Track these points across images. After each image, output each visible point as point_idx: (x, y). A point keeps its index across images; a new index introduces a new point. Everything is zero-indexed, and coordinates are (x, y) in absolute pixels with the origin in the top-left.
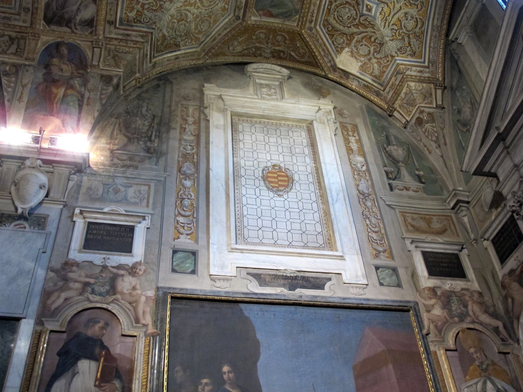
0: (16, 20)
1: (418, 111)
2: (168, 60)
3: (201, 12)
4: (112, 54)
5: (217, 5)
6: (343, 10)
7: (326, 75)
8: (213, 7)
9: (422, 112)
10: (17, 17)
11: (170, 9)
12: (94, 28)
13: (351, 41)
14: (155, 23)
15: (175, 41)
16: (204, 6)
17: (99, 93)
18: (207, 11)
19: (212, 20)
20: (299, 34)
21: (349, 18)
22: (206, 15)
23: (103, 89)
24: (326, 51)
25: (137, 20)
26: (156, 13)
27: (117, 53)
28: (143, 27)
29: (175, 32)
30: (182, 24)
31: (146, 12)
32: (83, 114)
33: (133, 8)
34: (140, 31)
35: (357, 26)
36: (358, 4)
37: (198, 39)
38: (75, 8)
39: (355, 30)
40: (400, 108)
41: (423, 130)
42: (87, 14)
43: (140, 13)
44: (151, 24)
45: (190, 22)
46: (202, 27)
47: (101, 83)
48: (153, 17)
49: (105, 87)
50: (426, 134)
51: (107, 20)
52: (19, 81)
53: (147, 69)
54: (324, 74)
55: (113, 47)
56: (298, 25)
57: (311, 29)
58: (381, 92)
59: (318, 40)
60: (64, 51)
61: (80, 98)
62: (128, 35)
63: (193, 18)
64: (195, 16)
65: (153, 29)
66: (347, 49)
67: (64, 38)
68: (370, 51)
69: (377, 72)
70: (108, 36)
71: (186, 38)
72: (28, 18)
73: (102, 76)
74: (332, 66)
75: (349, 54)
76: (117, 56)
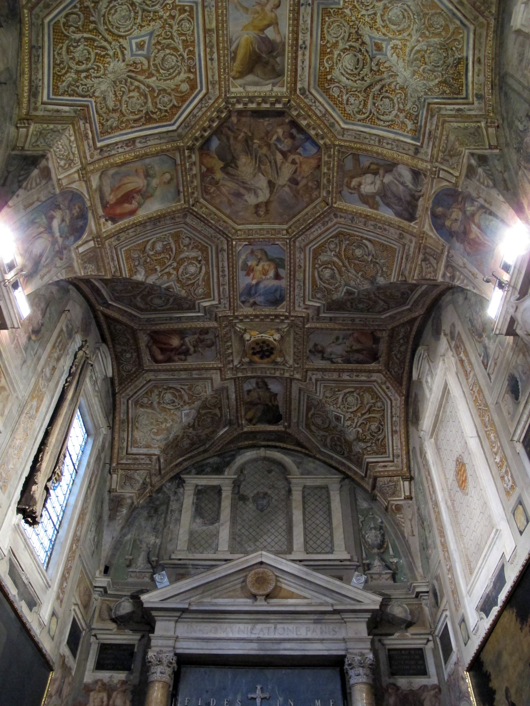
0: (409, 249)
2: (478, 76)
3: (417, 31)
4: (447, 158)
5: (408, 6)
8: (412, 12)
10: (407, 247)
11: (405, 77)
12: (421, 172)
14: (419, 98)
15: (452, 67)
16: (409, 26)
17: (482, 187)
18: (417, 21)
19: (431, 12)
22: (423, 21)
23: (479, 180)
25: (415, 119)
26: (409, 95)
27: (447, 152)
28: (422, 114)
29: (438, 66)
30: (429, 57)
31: (407, 108)
32: (499, 214)
33: (403, 122)
34: (426, 118)
37: (456, 31)
38: (401, 188)
42: (407, 176)
43: (409, 116)
44: (420, 102)
45: (428, 46)
46: (438, 26)
47: (473, 179)
48: (413, 99)
49: (478, 177)
51: (412, 154)
52: (460, 269)
53: (481, 109)
60: (440, 210)
61: (484, 210)
62: (430, 132)
63: (423, 41)
64: (420, 39)
65: (425, 101)
67: (427, 208)
70: (429, 157)
71: (452, 49)
73: (467, 176)
76: (449, 151)
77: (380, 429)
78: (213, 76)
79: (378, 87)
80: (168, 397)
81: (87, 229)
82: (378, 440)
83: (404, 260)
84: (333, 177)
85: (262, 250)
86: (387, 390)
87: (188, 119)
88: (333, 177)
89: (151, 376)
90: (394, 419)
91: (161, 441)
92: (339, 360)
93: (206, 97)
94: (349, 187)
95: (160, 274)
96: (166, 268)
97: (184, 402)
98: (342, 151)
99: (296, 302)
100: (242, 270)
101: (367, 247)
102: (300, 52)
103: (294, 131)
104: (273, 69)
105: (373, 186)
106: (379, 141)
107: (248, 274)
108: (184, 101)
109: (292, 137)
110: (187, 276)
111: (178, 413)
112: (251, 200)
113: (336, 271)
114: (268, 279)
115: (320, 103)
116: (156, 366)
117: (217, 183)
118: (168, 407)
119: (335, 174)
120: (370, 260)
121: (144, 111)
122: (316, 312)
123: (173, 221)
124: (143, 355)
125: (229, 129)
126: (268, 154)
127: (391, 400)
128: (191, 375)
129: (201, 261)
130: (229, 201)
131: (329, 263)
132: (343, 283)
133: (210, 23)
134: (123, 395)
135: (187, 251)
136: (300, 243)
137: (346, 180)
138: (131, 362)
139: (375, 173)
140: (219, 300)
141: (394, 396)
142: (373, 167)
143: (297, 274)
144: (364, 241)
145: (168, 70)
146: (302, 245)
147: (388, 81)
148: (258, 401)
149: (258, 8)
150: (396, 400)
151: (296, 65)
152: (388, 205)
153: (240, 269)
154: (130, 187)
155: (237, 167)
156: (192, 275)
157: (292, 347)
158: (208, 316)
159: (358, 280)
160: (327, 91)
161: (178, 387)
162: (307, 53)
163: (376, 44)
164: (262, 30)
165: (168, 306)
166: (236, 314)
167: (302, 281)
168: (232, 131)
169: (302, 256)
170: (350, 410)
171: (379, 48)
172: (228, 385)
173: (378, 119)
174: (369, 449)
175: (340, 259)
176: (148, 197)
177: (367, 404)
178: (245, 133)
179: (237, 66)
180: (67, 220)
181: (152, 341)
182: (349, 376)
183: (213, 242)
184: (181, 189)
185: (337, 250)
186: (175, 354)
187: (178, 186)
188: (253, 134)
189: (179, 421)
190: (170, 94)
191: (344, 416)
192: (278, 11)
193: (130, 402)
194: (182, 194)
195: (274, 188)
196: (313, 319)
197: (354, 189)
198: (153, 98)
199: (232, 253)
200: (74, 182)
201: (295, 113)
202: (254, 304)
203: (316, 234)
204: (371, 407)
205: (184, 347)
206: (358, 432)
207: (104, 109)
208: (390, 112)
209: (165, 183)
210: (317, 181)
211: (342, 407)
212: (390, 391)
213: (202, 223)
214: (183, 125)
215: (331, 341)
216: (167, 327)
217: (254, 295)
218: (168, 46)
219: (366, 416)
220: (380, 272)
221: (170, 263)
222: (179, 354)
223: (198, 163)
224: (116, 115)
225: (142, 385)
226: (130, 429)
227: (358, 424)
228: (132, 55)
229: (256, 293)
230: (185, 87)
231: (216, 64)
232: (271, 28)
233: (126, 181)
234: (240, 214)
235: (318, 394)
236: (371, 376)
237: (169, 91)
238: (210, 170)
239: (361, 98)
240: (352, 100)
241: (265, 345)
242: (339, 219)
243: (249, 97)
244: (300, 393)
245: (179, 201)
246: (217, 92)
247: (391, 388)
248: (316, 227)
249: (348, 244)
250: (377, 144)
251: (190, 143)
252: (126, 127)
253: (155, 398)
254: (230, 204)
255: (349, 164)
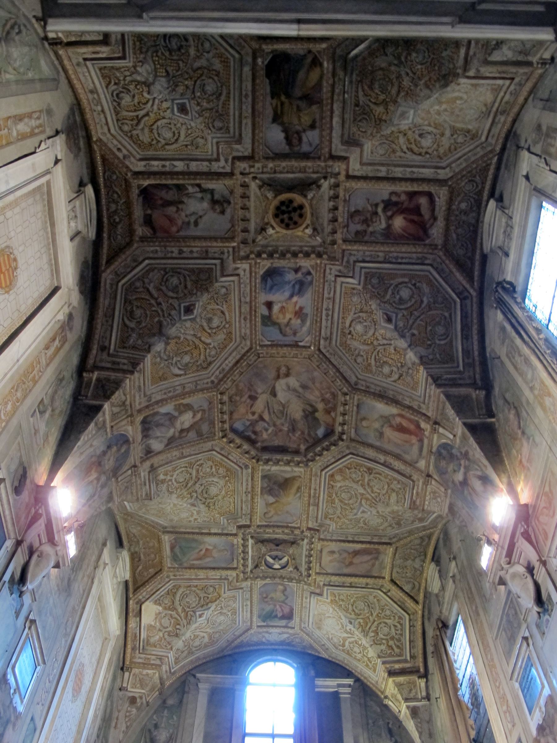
0: (140, 396)
1: (140, 695)
6: (193, 596)
7: (130, 599)
9: (141, 698)
10: (142, 396)
13: (169, 609)
14: (159, 496)
20: (161, 570)
21: (188, 602)
24: (152, 592)
31: (165, 485)
35: (183, 610)
36: (202, 606)
38: (158, 434)
39: (180, 610)
40: (134, 675)
41: (129, 709)
42: (156, 446)
43: (163, 482)
50: (128, 714)
54: (131, 596)
55: (134, 480)
56: (169, 568)
57: (168, 577)
58: (138, 651)
59: (159, 584)
62: (145, 485)
66: (160, 608)
67: (134, 443)
68: (167, 627)
69: (152, 640)
72: (143, 405)
74: (140, 600)
75: (158, 612)
77: (117, 98)
78: (316, 480)
79: (189, 485)
80: (427, 142)
81: (440, 443)
82: (115, 84)
83: (142, 386)
84: (218, 416)
85: (285, 335)
86: (119, 146)
87: (340, 457)
88: (218, 416)
89: (443, 174)
90: (99, 108)
91: (453, 91)
92: (191, 189)
93: (323, 467)
94: (204, 411)
95: (392, 342)
96: (384, 345)
97: (405, 135)
98: (211, 436)
99: (248, 275)
100: (307, 315)
101: (179, 369)
102: (250, 490)
103: (253, 437)
104: (270, 480)
105: (182, 420)
106: (182, 454)
107: (301, 309)
108: (340, 469)
109: (255, 433)
110: (365, 324)
111: (418, 121)
112: (293, 381)
113: (207, 328)
114: (280, 302)
115: (233, 462)
116: (432, 189)
117: (323, 400)
118: (430, 129)
119: (216, 418)
120: (175, 359)
121: (372, 476)
122: (225, 265)
123: (368, 384)
124: (444, 208)
125: (307, 441)
126: (275, 419)
127: (112, 135)
128: (388, 170)
129: (350, 333)
130: (314, 383)
131: (215, 333)
132: (198, 320)
133: (313, 510)
134: (489, 148)
135: (360, 350)
136: (246, 345)
137: (206, 415)
138: (462, 195)
139: (182, 431)
140: (335, 281)
141: (108, 139)
142: (184, 434)
143: (248, 309)
144: (182, 372)
145: (348, 492)
146: (244, 342)
147: (183, 491)
148: (300, 103)
149: (280, 513)
150: (104, 134)
151: (252, 484)
152: (168, 414)
153: (309, 316)
154: (396, 434)
155: (304, 411)
156: (360, 322)
157: (252, 209)
158: (352, 259)
159: (183, 331)
160: (228, 470)
161: (409, 155)
162: (244, 490)
163: (195, 506)
164: (277, 501)
165: (394, 282)
166: (318, 262)
167: (242, 303)
168: (305, 439)
169: (243, 331)
170: (168, 121)
171: (193, 505)
172: (340, 147)
173: (186, 467)
174: (128, 73)
175: (204, 343)
176: (386, 417)
177: (143, 129)
178: (294, 436)
179: (296, 484)
180: (451, 467)
181: (428, 226)
182: (175, 166)
183: (334, 351)
184: (355, 408)
185: (208, 350)
186: (402, 204)
187: (358, 412)
188: (288, 435)
189: (419, 112)
190: (350, 477)
191: (173, 114)
192: (265, 511)
193: (483, 138)
194: (356, 403)
195: (271, 391)
196: (228, 252)
197: (198, 412)
198: (363, 480)
199: (315, 337)
200: (435, 479)
201: (253, 453)
202: (297, 270)
203: (230, 359)
204: (137, 125)
205: (389, 213)
206: (149, 93)
207: (400, 496)
208: (178, 475)
209: (368, 419)
210: (231, 401)
211: (179, 125)
212: (115, 146)
213: (341, 370)
214: (344, 454)
215: (205, 218)
216: (403, 250)
217: (296, 283)
218: (345, 504)
219: (141, 113)
220: (162, 355)
221: (380, 347)
222: (396, 204)
223: (337, 424)
224: (392, 486)
225: (459, 162)
226: (496, 105)
227: (150, 103)
228: (371, 512)
229: (294, 286)
230: (338, 477)
231: (313, 486)
232: (271, 502)
233: (399, 442)
234: (304, 370)
235: (215, 141)
236: (145, 166)
237: (350, 480)
238: (327, 412)
239: (201, 474)
240: (208, 470)
241: (286, 221)
242: (209, 380)
243: (290, 466)
244: (240, 135)
245: (359, 400)
246: (314, 470)
247: (115, 150)
248: (230, 365)
249: (197, 361)
250: (184, 451)
251: (341, 443)
252: (388, 475)
253: (446, 142)
254: (313, 380)
255: (205, 428)
